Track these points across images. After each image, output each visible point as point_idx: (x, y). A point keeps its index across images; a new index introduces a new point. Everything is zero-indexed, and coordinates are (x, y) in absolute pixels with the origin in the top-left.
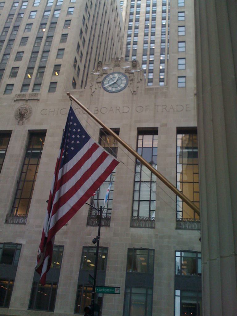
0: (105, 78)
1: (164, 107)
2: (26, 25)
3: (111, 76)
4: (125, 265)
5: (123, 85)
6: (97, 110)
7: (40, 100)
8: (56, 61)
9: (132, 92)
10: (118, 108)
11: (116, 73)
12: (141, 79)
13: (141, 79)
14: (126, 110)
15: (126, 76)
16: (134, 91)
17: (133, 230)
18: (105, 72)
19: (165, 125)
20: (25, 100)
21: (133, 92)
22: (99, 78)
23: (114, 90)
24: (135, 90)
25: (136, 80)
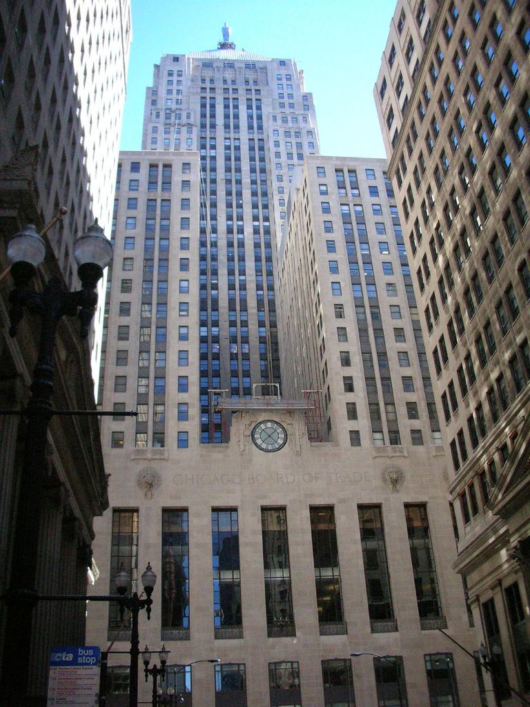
1: (339, 475)
3: (263, 426)
4: (321, 680)
5: (280, 442)
6: (252, 478)
10: (280, 476)
11: (269, 421)
14: (290, 479)
17: (323, 638)
19: (343, 501)
20: (146, 459)
23: (270, 447)
25: (297, 434)
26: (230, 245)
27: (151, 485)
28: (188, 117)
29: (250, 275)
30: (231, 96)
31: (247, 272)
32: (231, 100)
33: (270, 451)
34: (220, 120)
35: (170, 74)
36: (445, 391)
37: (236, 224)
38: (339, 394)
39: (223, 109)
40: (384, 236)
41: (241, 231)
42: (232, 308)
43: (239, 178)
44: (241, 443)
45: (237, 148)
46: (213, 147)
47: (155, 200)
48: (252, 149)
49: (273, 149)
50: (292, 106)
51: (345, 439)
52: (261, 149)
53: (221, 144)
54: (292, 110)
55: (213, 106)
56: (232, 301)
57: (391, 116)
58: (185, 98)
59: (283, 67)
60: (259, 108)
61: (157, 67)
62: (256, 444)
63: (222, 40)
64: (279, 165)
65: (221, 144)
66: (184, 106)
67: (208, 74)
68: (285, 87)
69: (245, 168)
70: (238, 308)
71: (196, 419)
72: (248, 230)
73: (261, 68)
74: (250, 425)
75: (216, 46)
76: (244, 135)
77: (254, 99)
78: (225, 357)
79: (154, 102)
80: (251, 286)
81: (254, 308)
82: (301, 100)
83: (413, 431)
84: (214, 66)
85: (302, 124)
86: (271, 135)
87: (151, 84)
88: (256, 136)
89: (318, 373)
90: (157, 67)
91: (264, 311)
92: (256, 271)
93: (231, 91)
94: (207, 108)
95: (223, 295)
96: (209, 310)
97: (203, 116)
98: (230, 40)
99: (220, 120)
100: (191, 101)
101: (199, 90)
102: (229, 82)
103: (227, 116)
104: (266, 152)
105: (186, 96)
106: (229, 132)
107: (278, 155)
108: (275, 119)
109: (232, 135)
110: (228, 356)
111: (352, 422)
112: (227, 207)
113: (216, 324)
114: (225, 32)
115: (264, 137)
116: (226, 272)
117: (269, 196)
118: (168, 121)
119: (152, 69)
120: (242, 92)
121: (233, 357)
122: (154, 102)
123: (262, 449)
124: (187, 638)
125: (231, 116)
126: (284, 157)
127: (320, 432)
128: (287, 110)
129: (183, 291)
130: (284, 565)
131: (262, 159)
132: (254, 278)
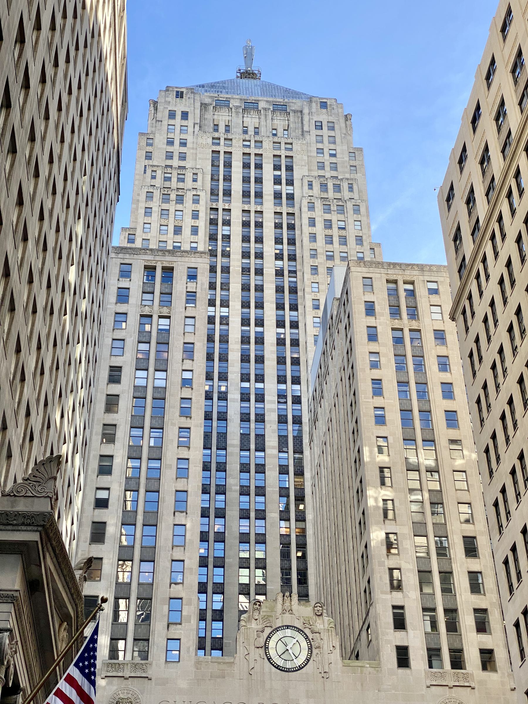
0: (269, 637)
2: (95, 489)
7: (153, 679)
8: (172, 589)
9: (320, 673)
11: (288, 627)
12: (333, 647)
13: (333, 647)
15: (307, 638)
16: (325, 672)
18: (268, 625)
21: (323, 672)
22: (258, 636)
23: (289, 665)
24: (327, 671)
25: (325, 647)
28: (195, 180)
29: (272, 402)
30: (253, 151)
31: (267, 398)
32: (253, 157)
33: (288, 671)
34: (237, 186)
35: (172, 115)
36: (518, 619)
38: (382, 592)
39: (241, 169)
40: (448, 374)
43: (259, 283)
44: (251, 657)
47: (151, 316)
48: (278, 226)
49: (307, 230)
50: (334, 167)
51: (390, 657)
52: (291, 227)
53: (237, 218)
54: (334, 173)
55: (228, 165)
56: (245, 438)
57: (457, 237)
58: (191, 151)
59: (324, 111)
60: (290, 168)
62: (269, 659)
63: (243, 69)
65: (237, 218)
66: (188, 164)
67: (222, 117)
68: (326, 139)
69: (268, 254)
70: (253, 447)
71: (192, 622)
73: (295, 112)
74: (263, 631)
77: (283, 157)
81: (273, 448)
82: (347, 159)
83: (483, 652)
84: (231, 106)
86: (305, 209)
89: (357, 565)
91: (287, 452)
92: (279, 396)
93: (253, 144)
96: (214, 448)
97: (214, 179)
98: (255, 67)
99: (237, 186)
100: (199, 156)
101: (210, 140)
102: (251, 131)
103: (246, 180)
104: (297, 232)
105: (193, 148)
106: (249, 202)
107: (313, 237)
108: (310, 185)
110: (237, 514)
111: (400, 634)
112: (243, 307)
114: (249, 55)
115: (296, 211)
116: (238, 397)
117: (300, 293)
118: (167, 184)
122: (149, 156)
123: (277, 667)
125: (253, 180)
128: (328, 173)
131: (292, 242)
132: (275, 406)
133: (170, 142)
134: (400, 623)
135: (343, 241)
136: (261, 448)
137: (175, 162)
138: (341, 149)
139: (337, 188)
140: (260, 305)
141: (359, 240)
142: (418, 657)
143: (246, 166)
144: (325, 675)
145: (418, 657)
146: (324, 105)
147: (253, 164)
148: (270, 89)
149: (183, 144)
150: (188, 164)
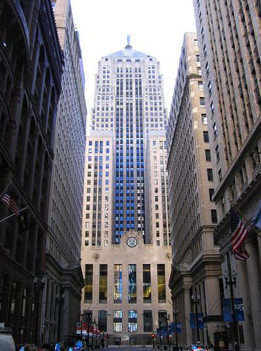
26: (128, 149)
27: (96, 258)
37: (130, 139)
41: (132, 143)
42: (128, 176)
45: (131, 104)
46: (122, 104)
48: (137, 104)
52: (141, 104)
56: (128, 172)
60: (140, 83)
61: (99, 62)
64: (147, 114)
66: (110, 84)
67: (120, 65)
72: (135, 142)
75: (122, 48)
76: (134, 98)
78: (125, 195)
79: (98, 82)
80: (135, 166)
85: (157, 92)
87: (97, 73)
88: (139, 98)
90: (99, 62)
94: (119, 83)
95: (125, 170)
109: (129, 98)
113: (122, 182)
119: (97, 64)
120: (133, 76)
121: (128, 195)
122: (98, 82)
124: (106, 303)
126: (149, 109)
127: (147, 240)
129: (107, 189)
130: (135, 282)
133: (104, 77)
134: (158, 235)
135: (156, 110)
136: (132, 176)
137: (106, 84)
138: (156, 75)
139: (155, 90)
140: (132, 131)
141: (160, 109)
142: (162, 244)
143: (127, 83)
144: (140, 248)
145: (162, 244)
146: (151, 60)
147: (129, 83)
148: (136, 54)
149: (108, 77)
150: (110, 84)
